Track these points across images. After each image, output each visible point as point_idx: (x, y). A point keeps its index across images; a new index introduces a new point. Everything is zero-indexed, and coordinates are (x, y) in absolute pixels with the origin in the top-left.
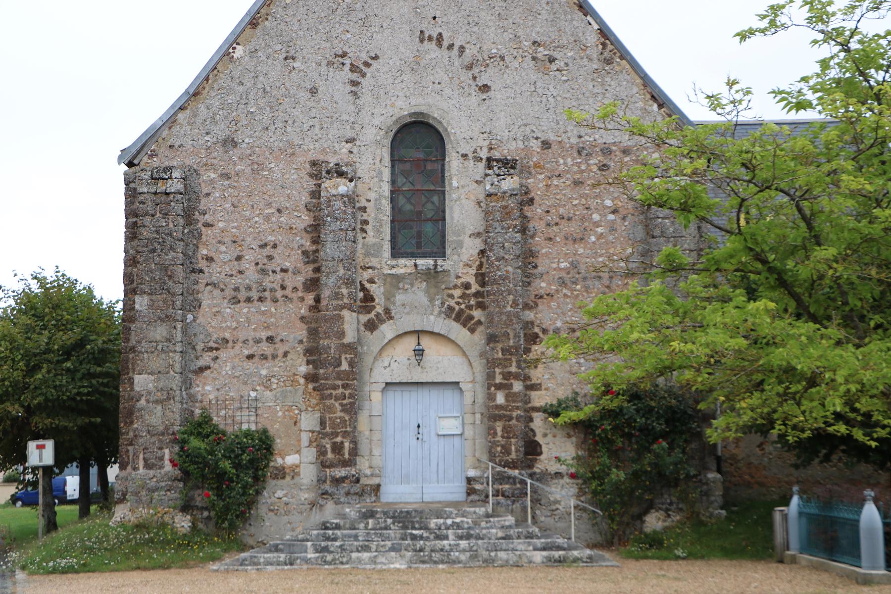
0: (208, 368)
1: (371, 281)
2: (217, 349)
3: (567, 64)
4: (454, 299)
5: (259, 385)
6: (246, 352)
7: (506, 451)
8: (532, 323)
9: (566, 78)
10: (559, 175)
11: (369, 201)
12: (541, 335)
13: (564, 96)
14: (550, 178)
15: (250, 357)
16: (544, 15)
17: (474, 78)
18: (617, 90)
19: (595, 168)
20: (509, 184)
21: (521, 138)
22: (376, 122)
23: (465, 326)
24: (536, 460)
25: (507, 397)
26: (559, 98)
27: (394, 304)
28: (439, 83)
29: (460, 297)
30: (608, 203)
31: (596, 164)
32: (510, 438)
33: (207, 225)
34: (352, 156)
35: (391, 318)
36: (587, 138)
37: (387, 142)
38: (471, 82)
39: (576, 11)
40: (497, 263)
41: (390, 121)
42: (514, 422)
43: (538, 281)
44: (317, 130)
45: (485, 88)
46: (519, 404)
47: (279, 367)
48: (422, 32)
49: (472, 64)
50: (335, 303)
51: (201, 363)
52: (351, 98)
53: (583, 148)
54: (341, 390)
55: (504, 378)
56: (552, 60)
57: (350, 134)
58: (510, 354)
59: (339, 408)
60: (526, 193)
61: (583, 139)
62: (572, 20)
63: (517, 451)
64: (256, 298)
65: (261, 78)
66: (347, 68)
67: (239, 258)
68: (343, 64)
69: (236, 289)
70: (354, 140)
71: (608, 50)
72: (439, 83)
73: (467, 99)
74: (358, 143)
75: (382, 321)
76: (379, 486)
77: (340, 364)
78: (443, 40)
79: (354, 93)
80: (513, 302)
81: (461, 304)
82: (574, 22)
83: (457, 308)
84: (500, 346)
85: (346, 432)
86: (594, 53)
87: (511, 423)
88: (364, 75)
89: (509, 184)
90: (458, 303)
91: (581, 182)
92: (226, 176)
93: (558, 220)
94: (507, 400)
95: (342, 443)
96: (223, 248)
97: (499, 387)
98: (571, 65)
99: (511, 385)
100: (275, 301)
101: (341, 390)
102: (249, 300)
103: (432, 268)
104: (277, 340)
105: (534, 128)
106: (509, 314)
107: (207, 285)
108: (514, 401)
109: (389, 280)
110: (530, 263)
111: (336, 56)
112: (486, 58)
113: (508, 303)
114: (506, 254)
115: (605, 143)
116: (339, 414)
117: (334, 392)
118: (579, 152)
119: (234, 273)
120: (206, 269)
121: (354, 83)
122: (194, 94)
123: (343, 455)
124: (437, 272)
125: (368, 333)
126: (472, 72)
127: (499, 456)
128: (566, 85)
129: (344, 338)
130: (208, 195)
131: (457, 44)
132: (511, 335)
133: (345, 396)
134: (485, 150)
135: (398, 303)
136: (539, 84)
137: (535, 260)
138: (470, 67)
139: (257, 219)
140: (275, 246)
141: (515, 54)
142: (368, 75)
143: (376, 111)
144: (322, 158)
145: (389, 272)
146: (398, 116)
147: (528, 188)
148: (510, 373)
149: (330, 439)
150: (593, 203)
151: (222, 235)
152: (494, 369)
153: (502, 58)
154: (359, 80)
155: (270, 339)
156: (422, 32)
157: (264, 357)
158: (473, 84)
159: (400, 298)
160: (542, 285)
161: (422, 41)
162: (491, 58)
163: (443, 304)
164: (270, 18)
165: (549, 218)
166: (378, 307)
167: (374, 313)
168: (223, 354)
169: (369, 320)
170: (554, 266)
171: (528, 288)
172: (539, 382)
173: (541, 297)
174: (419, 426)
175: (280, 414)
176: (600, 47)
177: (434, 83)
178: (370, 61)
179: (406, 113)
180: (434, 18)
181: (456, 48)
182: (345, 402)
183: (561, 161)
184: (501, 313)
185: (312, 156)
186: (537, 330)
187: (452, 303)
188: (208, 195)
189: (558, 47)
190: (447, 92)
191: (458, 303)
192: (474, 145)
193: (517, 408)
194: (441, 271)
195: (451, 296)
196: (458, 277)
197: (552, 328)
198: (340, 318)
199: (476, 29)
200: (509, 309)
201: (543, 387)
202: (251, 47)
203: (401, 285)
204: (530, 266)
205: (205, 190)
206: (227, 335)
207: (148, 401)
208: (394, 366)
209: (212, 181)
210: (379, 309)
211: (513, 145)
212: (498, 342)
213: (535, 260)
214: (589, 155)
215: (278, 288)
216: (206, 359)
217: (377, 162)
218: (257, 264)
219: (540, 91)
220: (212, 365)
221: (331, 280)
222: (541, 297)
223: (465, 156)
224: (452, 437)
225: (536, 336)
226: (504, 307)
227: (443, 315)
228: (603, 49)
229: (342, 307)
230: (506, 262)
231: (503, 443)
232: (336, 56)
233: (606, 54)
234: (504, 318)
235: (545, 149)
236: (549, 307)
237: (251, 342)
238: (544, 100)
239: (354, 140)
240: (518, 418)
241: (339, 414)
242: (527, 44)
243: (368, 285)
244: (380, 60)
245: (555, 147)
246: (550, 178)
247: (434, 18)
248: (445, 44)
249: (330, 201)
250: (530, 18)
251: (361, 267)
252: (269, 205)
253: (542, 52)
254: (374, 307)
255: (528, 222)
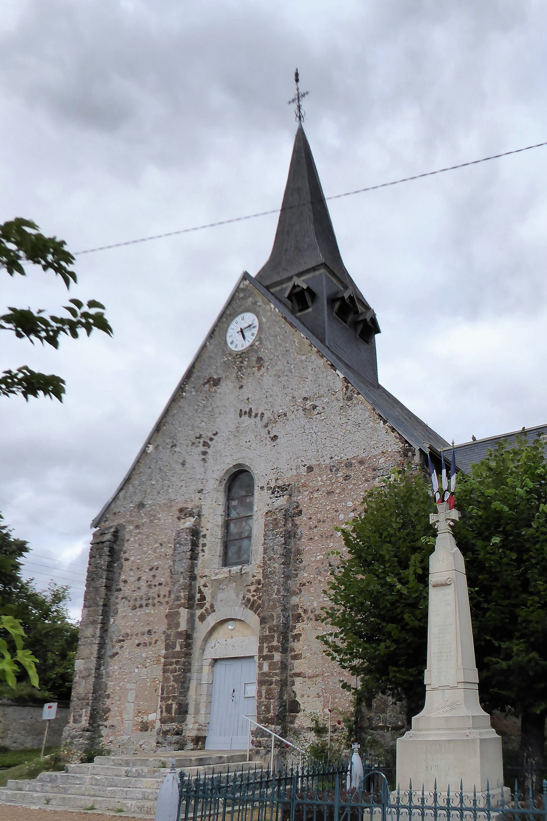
0: (117, 654)
1: (205, 586)
2: (123, 641)
3: (323, 408)
4: (250, 593)
5: (140, 664)
6: (137, 642)
7: (268, 710)
8: (297, 606)
9: (324, 418)
10: (318, 490)
11: (207, 530)
12: (303, 615)
13: (322, 431)
14: (312, 493)
15: (138, 645)
16: (310, 378)
17: (269, 432)
18: (356, 418)
19: (341, 479)
20: (282, 501)
21: (295, 468)
22: (215, 476)
23: (255, 612)
24: (296, 716)
25: (270, 665)
26: (319, 433)
27: (216, 600)
28: (249, 441)
29: (254, 591)
30: (350, 504)
31: (342, 476)
32: (270, 699)
33: (127, 560)
34: (200, 501)
35: (214, 611)
36: (336, 458)
37: (222, 488)
38: (266, 436)
39: (329, 370)
40: (268, 562)
41: (222, 474)
42: (273, 686)
43: (302, 572)
44: (184, 488)
45: (275, 438)
46: (277, 671)
47: (152, 651)
48: (241, 410)
49: (268, 424)
50: (176, 603)
51: (114, 651)
52: (202, 463)
53: (333, 466)
54: (174, 666)
55: (270, 651)
56: (315, 407)
57: (200, 487)
58: (273, 632)
59: (172, 678)
60: (297, 507)
61: (333, 459)
62: (327, 376)
63: (274, 709)
64: (144, 604)
65: (159, 462)
66: (201, 445)
67: (139, 579)
68: (199, 442)
69: (136, 600)
70: (202, 490)
71: (349, 390)
72: (249, 441)
73: (264, 448)
74: (204, 492)
75: (209, 614)
76: (205, 737)
77: (175, 647)
78: (252, 412)
79: (204, 460)
80: (277, 591)
81: (255, 596)
82: (328, 378)
83: (252, 599)
84: (267, 626)
85: (175, 696)
86: (340, 395)
87: (271, 687)
88: (209, 446)
89: (282, 501)
90: (253, 596)
91: (332, 492)
92: (137, 527)
93: (316, 524)
94: (270, 669)
95: (172, 704)
96: (132, 573)
97: (265, 658)
98: (326, 407)
99: (273, 656)
100: (154, 605)
101: (174, 666)
102: (141, 606)
103: (239, 571)
104: (152, 633)
105: (303, 459)
106: (274, 600)
107: (123, 598)
108: (274, 669)
109: (214, 583)
110: (298, 559)
111: (197, 438)
112: (276, 417)
113: (274, 592)
114: (275, 554)
115: (348, 459)
116: (172, 683)
117: (170, 667)
118: (331, 470)
119: (135, 589)
120: (122, 588)
121: (205, 453)
122: (128, 480)
123: (171, 714)
124: (242, 574)
125: (200, 623)
126: (268, 429)
127: (263, 714)
128: (323, 423)
129: (179, 627)
130: (128, 540)
131: (260, 412)
132: (275, 618)
133: (176, 670)
134: (274, 481)
135: (219, 599)
136: (306, 427)
137: (301, 557)
138: (266, 426)
139: (150, 552)
140: (157, 569)
141: (293, 409)
142: (212, 446)
143: (215, 469)
144: (185, 506)
145: (215, 578)
146: (227, 468)
147: (298, 503)
148: (273, 646)
149: (165, 702)
150: (339, 506)
151: (133, 564)
152: (263, 644)
153: (285, 415)
154: (207, 450)
155: (149, 632)
156: (241, 410)
157: (145, 645)
158: (268, 436)
159: (220, 596)
160: (304, 576)
161: (241, 416)
162: (279, 416)
163: (244, 597)
164: (166, 424)
165: (311, 523)
166: (207, 603)
167: (204, 608)
168: (125, 644)
169: (202, 613)
170: (313, 559)
171: (296, 579)
172: (300, 652)
173: (304, 585)
174: (234, 691)
175: (149, 684)
176: (345, 389)
177: (246, 442)
178: (213, 437)
179: (231, 466)
180: (248, 399)
181: (259, 415)
182: (175, 674)
183: (319, 479)
184: (269, 600)
185: (180, 506)
186: (300, 611)
187: (249, 596)
188: (128, 540)
189: (318, 397)
190: (254, 445)
191: (253, 596)
192: (267, 478)
193: (276, 674)
194: (244, 573)
195: (249, 591)
196: (254, 576)
197: (310, 608)
198: (178, 613)
199: (270, 399)
200: (274, 596)
201: (303, 657)
202: (156, 444)
203: (221, 587)
204: (297, 562)
205: (127, 538)
206: (128, 631)
207: (80, 677)
208: (218, 645)
209: (131, 531)
210: (207, 606)
211: (290, 474)
212: (266, 623)
213: (301, 557)
214: (337, 470)
215: (156, 597)
216: (117, 649)
217: (214, 502)
218: (147, 581)
219: (307, 431)
220: (119, 652)
221: (176, 588)
222: (304, 585)
223: (262, 488)
224: (252, 698)
225: (300, 616)
226: (272, 595)
227: (244, 606)
228: (347, 390)
229: (179, 606)
230: (274, 560)
231: (265, 703)
232: (197, 438)
233: (349, 394)
234: (271, 603)
235: (309, 472)
236: (309, 591)
237: (139, 635)
238: (310, 437)
239: (202, 490)
240: (277, 682)
241: (172, 683)
242: (299, 400)
243: (203, 589)
244: (218, 435)
245: (316, 470)
246: (312, 493)
247: (248, 399)
248: (253, 414)
249: (179, 533)
250: (302, 382)
251: (200, 577)
252: (156, 542)
253: (309, 403)
254: (205, 604)
255: (297, 528)
